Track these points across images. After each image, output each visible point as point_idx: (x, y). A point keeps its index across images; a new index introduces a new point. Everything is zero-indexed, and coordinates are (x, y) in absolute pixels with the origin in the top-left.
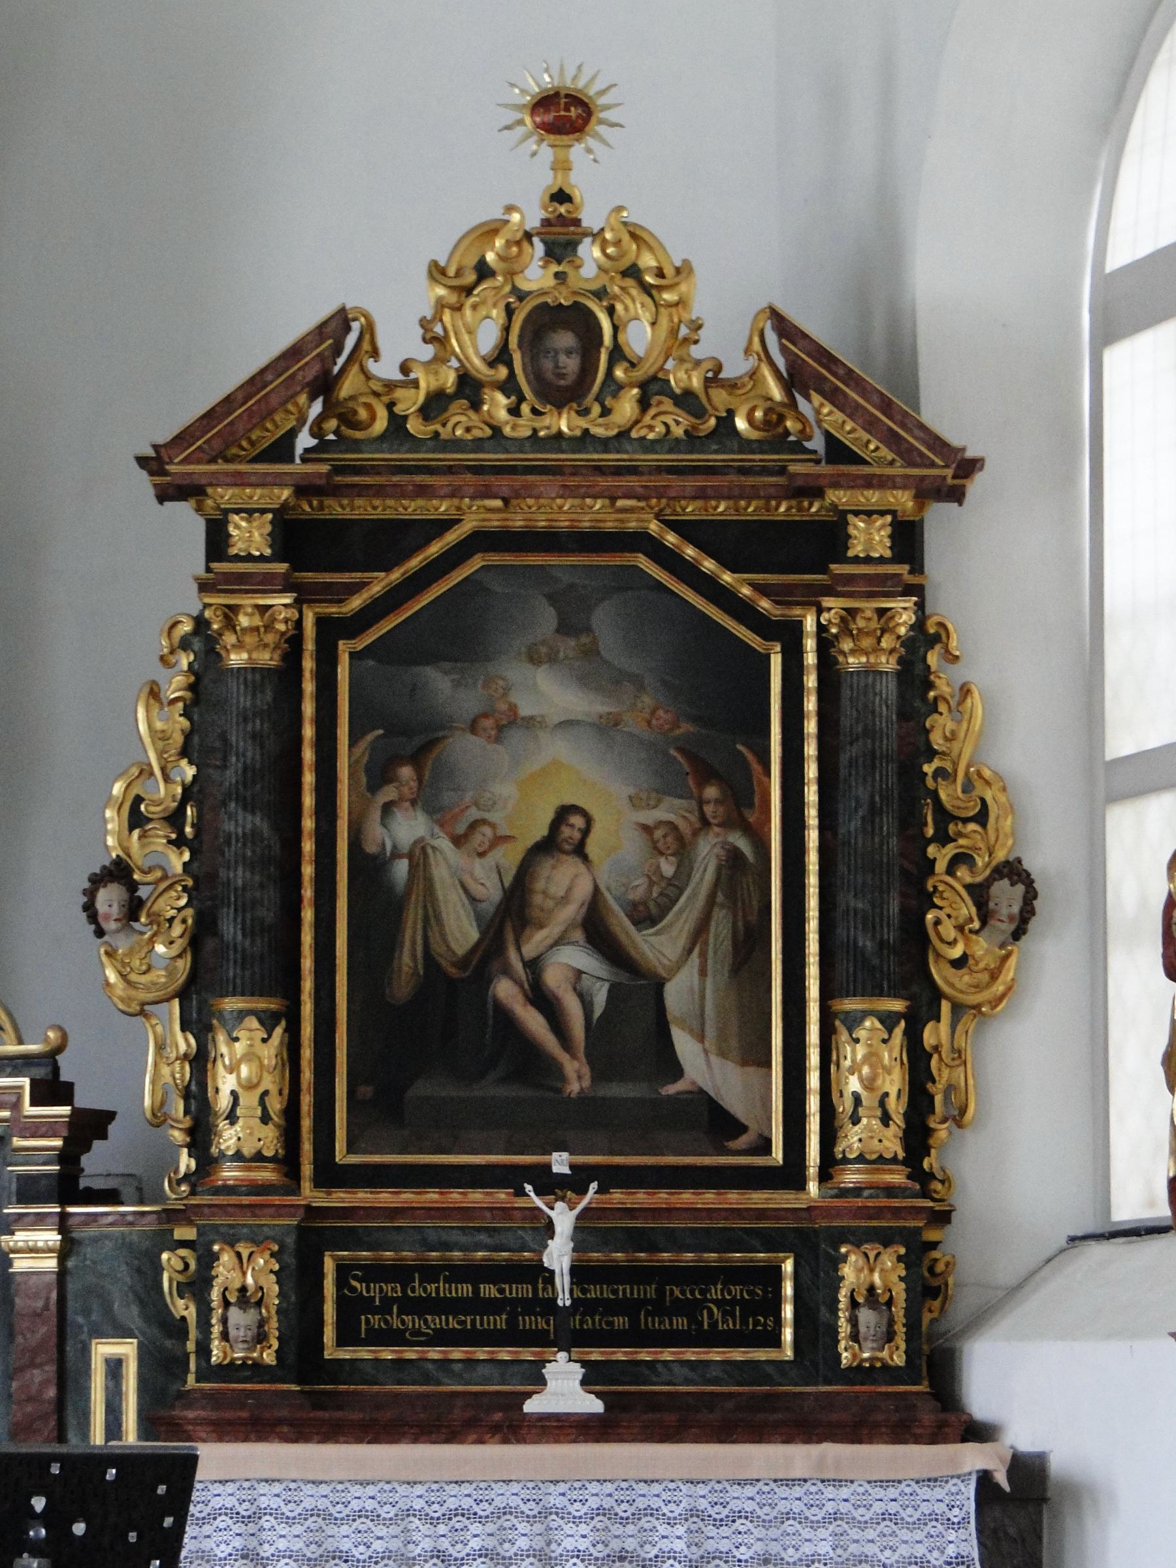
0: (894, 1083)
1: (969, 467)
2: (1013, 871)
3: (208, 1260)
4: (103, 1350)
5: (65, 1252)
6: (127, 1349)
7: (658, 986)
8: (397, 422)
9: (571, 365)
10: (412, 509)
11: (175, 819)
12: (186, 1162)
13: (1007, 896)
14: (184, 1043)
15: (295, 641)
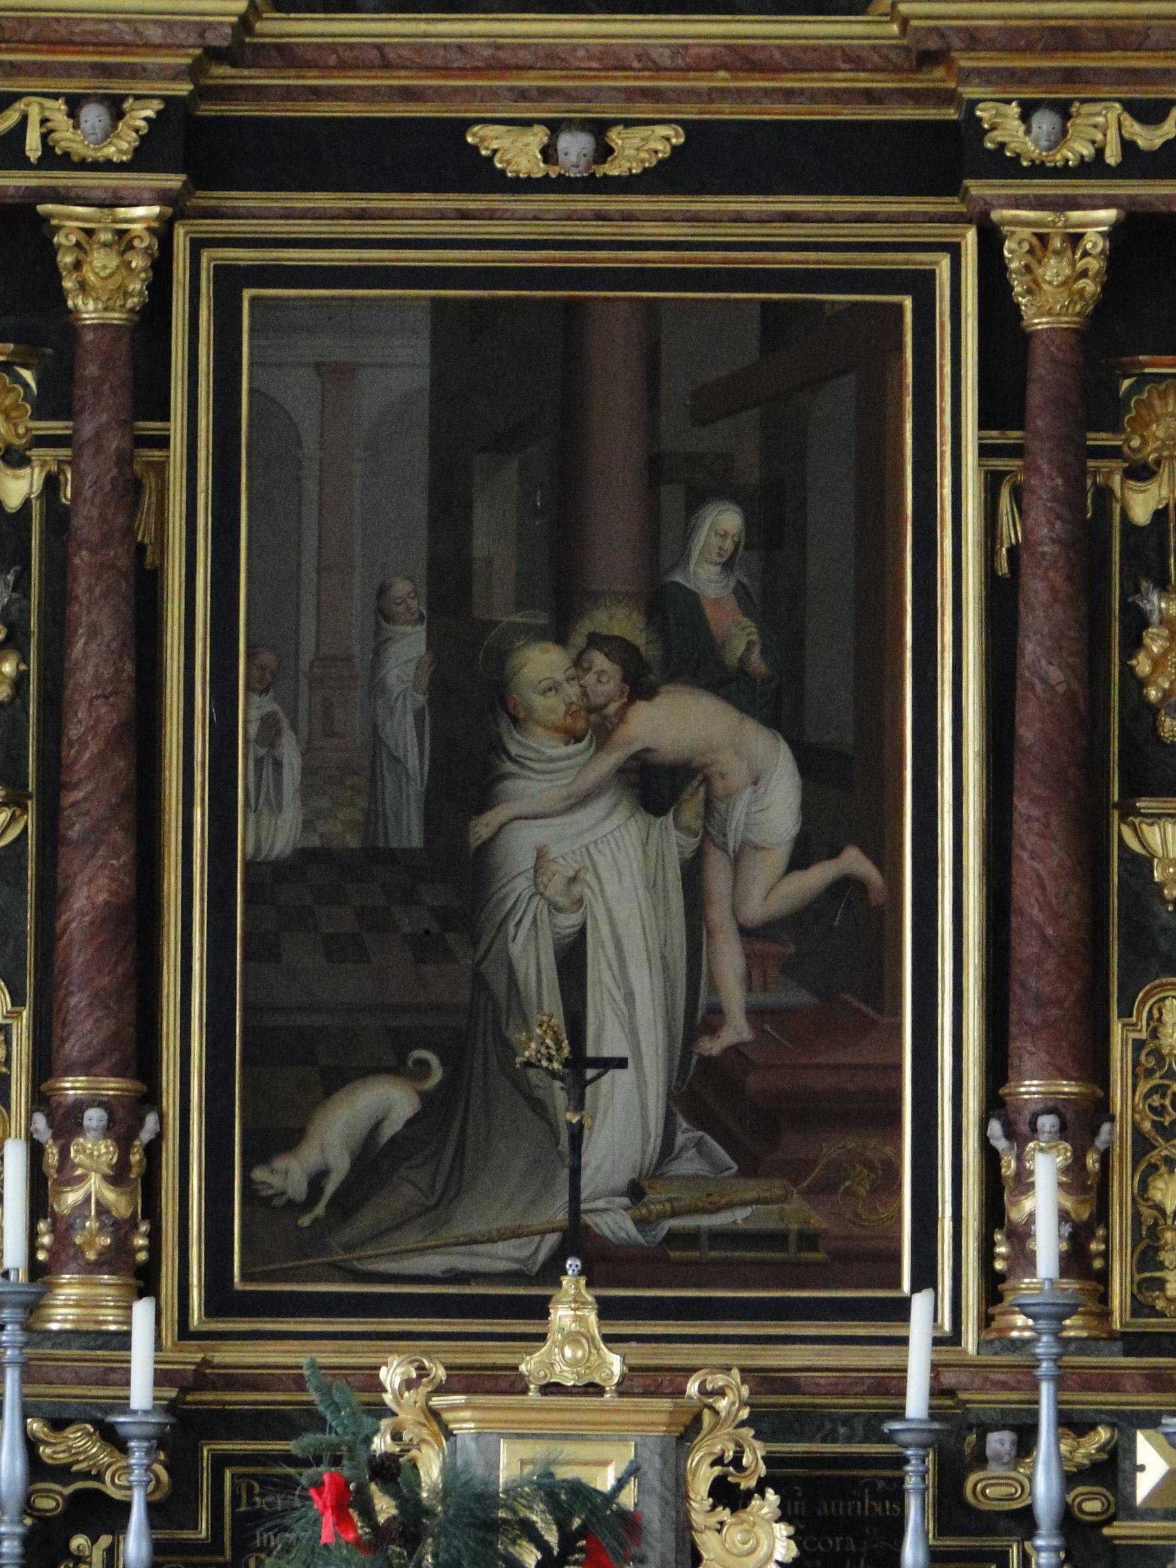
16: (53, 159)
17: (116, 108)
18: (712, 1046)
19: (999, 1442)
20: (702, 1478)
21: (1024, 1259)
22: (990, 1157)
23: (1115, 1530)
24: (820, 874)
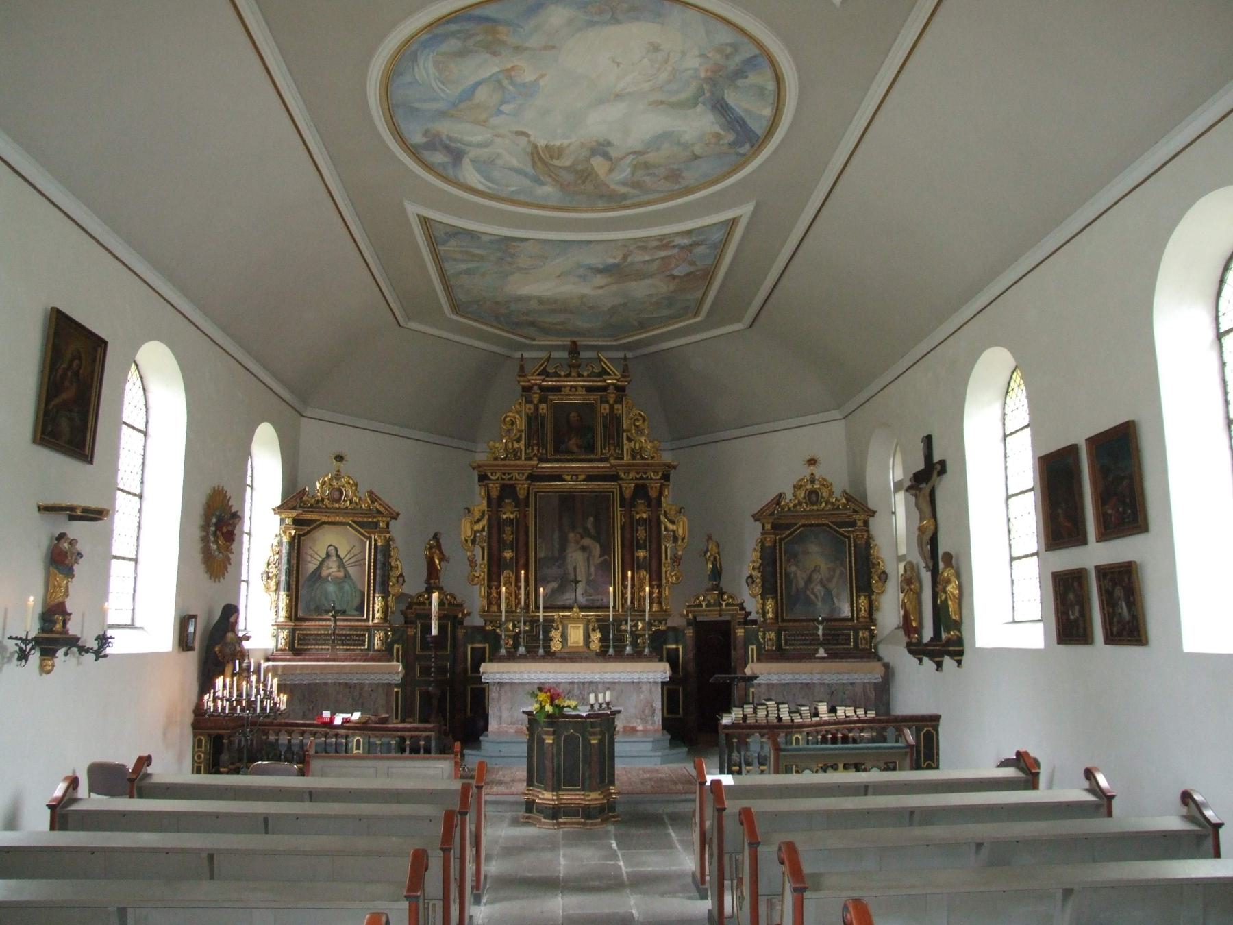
0: (867, 606)
1: (874, 512)
2: (884, 573)
3: (764, 634)
4: (750, 647)
5: (744, 633)
6: (754, 647)
7: (831, 591)
8: (789, 509)
9: (815, 499)
10: (793, 521)
11: (759, 568)
12: (762, 619)
13: (883, 577)
14: (761, 601)
15: (775, 542)
16: (516, 480)
17: (523, 474)
18: (591, 578)
19: (623, 623)
20: (591, 627)
21: (626, 602)
22: (622, 591)
23: (637, 633)
24: (602, 559)
